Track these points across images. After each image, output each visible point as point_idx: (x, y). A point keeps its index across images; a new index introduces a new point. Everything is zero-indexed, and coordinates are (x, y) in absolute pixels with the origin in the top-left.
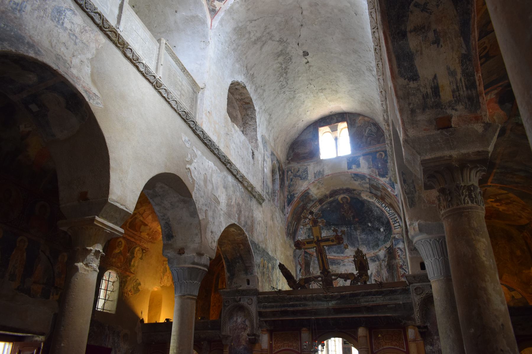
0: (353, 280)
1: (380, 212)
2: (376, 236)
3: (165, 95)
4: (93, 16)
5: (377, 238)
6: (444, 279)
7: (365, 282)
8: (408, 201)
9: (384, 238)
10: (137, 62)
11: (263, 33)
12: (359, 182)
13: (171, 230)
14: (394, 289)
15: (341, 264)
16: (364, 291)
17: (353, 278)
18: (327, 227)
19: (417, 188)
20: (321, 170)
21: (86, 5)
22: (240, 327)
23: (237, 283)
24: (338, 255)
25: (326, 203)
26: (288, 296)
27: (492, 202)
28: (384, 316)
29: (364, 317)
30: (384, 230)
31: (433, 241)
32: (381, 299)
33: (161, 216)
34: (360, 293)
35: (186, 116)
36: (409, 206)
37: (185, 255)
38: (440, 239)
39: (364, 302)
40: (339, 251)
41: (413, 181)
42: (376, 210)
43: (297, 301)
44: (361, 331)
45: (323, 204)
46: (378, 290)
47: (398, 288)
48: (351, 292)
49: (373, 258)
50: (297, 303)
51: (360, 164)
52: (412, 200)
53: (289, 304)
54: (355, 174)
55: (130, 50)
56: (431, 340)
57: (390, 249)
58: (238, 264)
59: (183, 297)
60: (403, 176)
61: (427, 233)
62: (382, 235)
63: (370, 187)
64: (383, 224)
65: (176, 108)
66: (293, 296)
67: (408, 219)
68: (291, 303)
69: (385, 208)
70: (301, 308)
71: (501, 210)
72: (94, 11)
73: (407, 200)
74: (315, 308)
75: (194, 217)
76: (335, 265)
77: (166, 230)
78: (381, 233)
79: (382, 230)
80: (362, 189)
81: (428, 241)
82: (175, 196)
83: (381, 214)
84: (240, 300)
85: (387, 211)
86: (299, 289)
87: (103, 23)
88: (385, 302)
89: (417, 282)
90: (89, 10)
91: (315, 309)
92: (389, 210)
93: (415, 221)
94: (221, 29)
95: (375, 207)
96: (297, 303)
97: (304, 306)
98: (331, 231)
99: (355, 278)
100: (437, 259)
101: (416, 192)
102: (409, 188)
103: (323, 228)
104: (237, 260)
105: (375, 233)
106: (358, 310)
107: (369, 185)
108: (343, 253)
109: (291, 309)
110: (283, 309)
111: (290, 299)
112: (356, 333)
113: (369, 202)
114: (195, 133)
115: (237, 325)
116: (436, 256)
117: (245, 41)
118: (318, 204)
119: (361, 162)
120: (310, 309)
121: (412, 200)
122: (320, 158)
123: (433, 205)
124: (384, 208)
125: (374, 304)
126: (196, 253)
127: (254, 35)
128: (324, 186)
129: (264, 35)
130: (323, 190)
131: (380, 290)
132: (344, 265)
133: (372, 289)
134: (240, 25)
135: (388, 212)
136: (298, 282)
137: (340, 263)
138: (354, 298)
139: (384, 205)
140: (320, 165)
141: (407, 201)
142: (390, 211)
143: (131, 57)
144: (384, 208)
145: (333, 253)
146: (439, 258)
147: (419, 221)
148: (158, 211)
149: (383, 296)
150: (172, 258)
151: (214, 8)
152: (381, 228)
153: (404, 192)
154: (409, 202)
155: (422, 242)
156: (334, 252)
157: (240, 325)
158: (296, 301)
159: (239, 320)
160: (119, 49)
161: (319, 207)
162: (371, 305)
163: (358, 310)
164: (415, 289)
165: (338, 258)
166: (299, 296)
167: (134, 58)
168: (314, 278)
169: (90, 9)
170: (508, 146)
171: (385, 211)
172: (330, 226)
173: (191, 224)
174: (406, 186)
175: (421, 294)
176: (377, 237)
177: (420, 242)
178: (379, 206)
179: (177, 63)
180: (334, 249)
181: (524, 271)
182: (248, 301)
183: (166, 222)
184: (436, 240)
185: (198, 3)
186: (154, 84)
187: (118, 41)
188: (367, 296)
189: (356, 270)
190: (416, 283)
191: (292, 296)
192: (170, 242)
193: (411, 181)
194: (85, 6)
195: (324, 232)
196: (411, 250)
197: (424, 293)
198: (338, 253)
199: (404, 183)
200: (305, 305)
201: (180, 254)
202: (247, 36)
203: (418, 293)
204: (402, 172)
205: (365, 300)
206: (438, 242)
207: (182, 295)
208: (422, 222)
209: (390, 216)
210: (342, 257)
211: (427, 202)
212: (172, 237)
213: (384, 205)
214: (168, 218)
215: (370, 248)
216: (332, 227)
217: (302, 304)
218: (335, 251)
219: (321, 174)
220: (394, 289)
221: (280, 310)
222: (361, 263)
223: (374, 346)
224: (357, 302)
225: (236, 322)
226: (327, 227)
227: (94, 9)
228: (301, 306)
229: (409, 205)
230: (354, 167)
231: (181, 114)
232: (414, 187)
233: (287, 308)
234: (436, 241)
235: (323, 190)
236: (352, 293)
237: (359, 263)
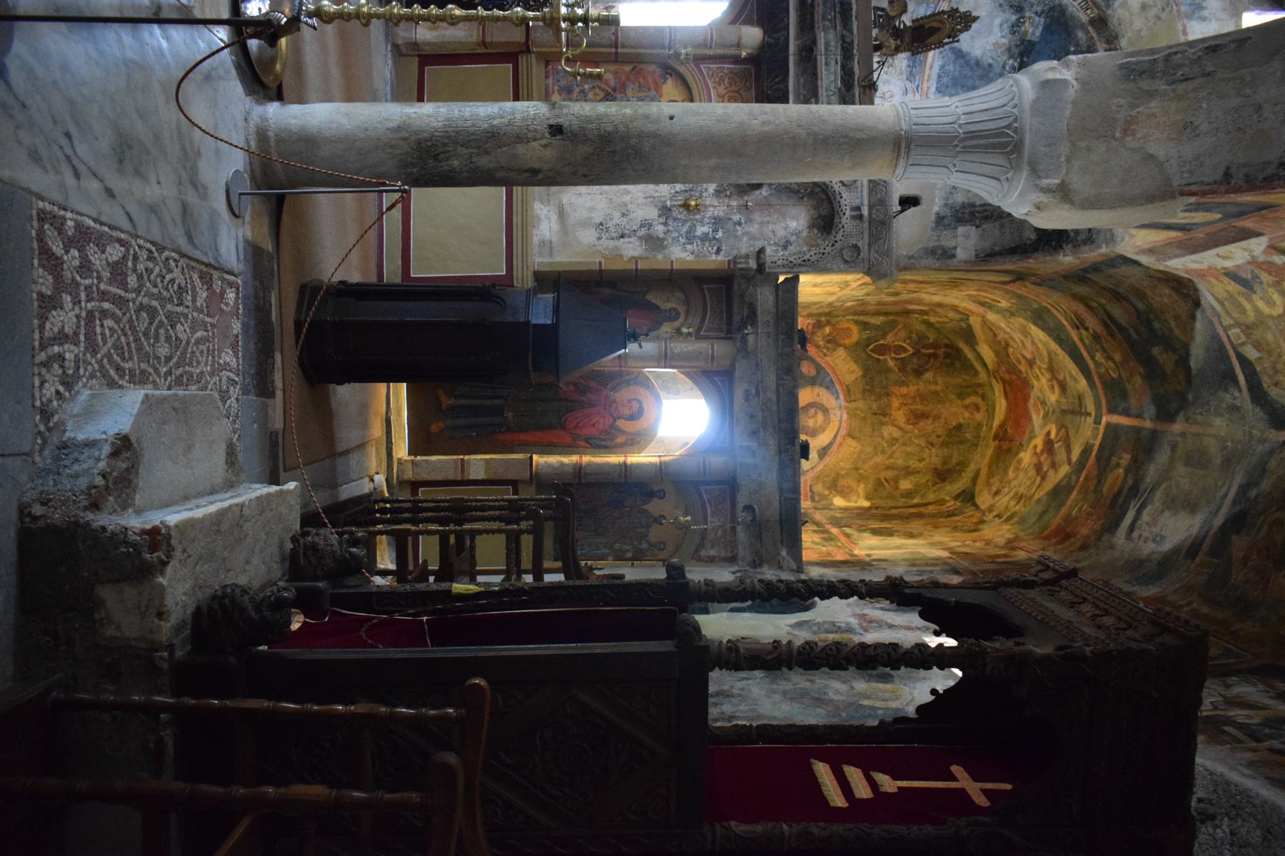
0: (887, 13)
6: (902, 130)
7: (877, 48)
8: (1143, 61)
15: (909, 85)
16: (856, 42)
17: (893, 14)
18: (1017, 46)
19: (1181, 87)
20: (1205, 13)
24: (934, 77)
25: (1092, 38)
27: (1049, 433)
28: (788, 91)
29: (787, 39)
31: (1012, 112)
32: (833, 85)
34: (851, 31)
36: (1124, 61)
38: (1016, 131)
39: (826, 39)
40: (945, 80)
41: (1209, 74)
44: (753, 35)
45: (1090, 28)
46: (856, 78)
48: (854, 7)
52: (1144, 72)
56: (728, 194)
60: (1233, 41)
61: (1035, 102)
71: (1022, 455)
73: (1146, 58)
76: (909, 66)
81: (1013, 99)
88: (825, 94)
93: (1077, 73)
98: (1005, 58)
99: (893, 18)
100: (959, 118)
102: (1187, 62)
103: (1015, 32)
106: (807, 25)
108: (939, 92)
112: (748, 22)
116: (966, 119)
118: (1093, 13)
121: (1144, 72)
122: (1247, 9)
123: (1118, 130)
125: (819, 63)
128: (1150, 24)
130: (1138, 23)
131: (856, 82)
132: (906, 92)
137: (911, 81)
138: (838, 15)
140: (1224, 9)
145: (940, 63)
146: (960, 126)
147: (1075, 83)
149: (839, 89)
153: (1174, 50)
154: (1137, 63)
156: (942, 67)
161: (1083, 17)
162: (819, 57)
163: (807, 25)
165: (926, 77)
170: (1229, 444)
172: (1019, 54)
174: (1194, 54)
180: (951, 67)
181: (862, 486)
184: (1015, 120)
188: (843, 48)
189: (913, 21)
193: (1210, 68)
195: (1003, 37)
197: (842, 188)
198: (939, 77)
199: (1207, 48)
205: (832, 43)
206: (1008, 127)
208: (1071, 93)
210: (928, 88)
211: (1134, 113)
216: (1015, 61)
218: (947, 67)
219: (1194, 12)
222: (933, 31)
223: (716, 66)
224: (827, 23)
226: (1017, 46)
229: (1128, 63)
232: (1186, 80)
234: (1012, 119)
235: (1138, 23)
236: (851, 9)
237: (935, 24)
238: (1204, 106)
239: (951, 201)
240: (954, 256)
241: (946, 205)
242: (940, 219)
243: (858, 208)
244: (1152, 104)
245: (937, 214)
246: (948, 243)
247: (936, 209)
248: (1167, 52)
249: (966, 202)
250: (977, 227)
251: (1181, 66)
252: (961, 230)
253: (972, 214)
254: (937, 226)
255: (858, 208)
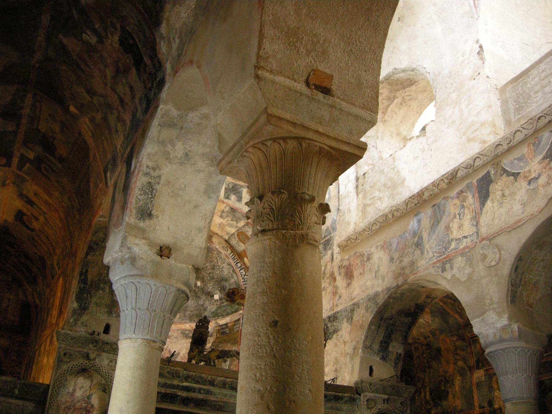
1: (229, 272)
2: (202, 303)
5: (203, 305)
8: (511, 295)
9: (216, 310)
12: (224, 222)
13: (151, 201)
14: (340, 394)
19: (523, 283)
22: (78, 405)
23: (86, 326)
26: (185, 372)
30: (221, 299)
33: (147, 167)
37: (172, 261)
42: (223, 267)
43: (197, 382)
47: (346, 395)
49: (187, 332)
50: (195, 385)
51: (242, 197)
53: (181, 384)
54: (232, 209)
57: (224, 327)
58: (101, 292)
59: (153, 344)
62: (213, 305)
63: (234, 233)
64: (222, 289)
66: (194, 374)
67: (508, 318)
68: (185, 384)
69: (241, 270)
70: (200, 396)
73: (510, 293)
74: (224, 400)
75: (210, 197)
77: (141, 197)
78: (213, 301)
79: (216, 297)
80: (219, 232)
82: (209, 143)
83: (230, 275)
84: (94, 359)
85: (241, 275)
86: (202, 364)
89: (371, 391)
91: (224, 402)
92: (244, 274)
93: (514, 322)
95: (224, 263)
96: (195, 385)
97: (206, 394)
101: (520, 286)
104: (102, 285)
105: (204, 297)
107: (238, 230)
109: (184, 394)
110: (169, 391)
111: (187, 378)
113: (219, 253)
115: (72, 401)
119: (243, 196)
120: (216, 401)
124: (239, 269)
126: (193, 266)
133: (345, 393)
135: (243, 276)
136: (205, 353)
139: (239, 265)
141: (509, 294)
142: (246, 277)
144: (239, 269)
147: (518, 324)
148: (148, 154)
150: (142, 258)
152: (216, 294)
153: (510, 282)
155: (516, 350)
157: (79, 401)
158: (196, 383)
159: (79, 394)
164: (367, 401)
166: (203, 375)
168: (235, 353)
171: (240, 274)
173: (196, 207)
175: (372, 408)
176: (204, 304)
177: (514, 350)
178: (233, 264)
182: (111, 364)
183: (150, 183)
190: (370, 392)
191: (191, 373)
192: (142, 224)
193: (521, 272)
196: (366, 348)
197: (376, 407)
200: (208, 392)
201: (161, 256)
203: (370, 406)
204: (520, 257)
207: (152, 339)
208: (521, 326)
209: (244, 283)
211: (525, 303)
212: (150, 215)
213: (239, 265)
214: (159, 177)
215: (185, 316)
217: (204, 390)
220: (340, 394)
221: (163, 391)
225: (72, 394)
228: (201, 393)
230: (233, 197)
233: (177, 391)
238: (531, 276)
239: (377, 351)
240: (400, 354)
241: (378, 354)
242: (384, 358)
243: (384, 400)
244: (524, 294)
245: (380, 359)
246: (393, 356)
247: (378, 359)
248: (510, 285)
249: (379, 344)
250: (392, 341)
251: (516, 281)
252: (390, 349)
253: (385, 342)
254: (386, 360)
255: (384, 400)
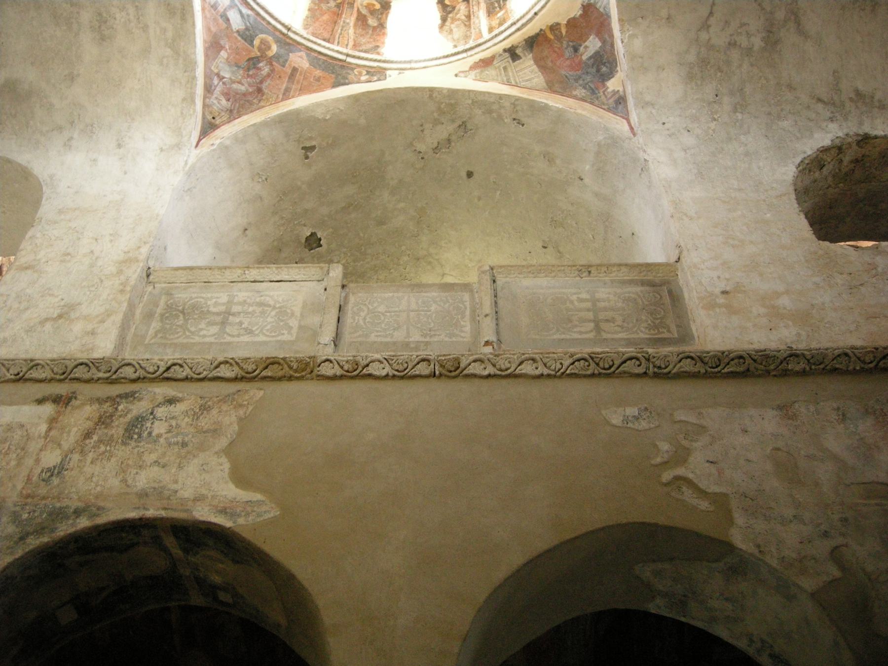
3: (490, 370)
4: (215, 375)
10: (360, 369)
11: (763, 9)
21: (193, 370)
35: (593, 365)
55: (327, 363)
65: (546, 371)
72: (212, 367)
87: (242, 368)
90: (205, 373)
94: (654, 111)
114: (669, 378)
117: (745, 66)
127: (749, 35)
129: (768, 9)
134: (691, 57)
143: (339, 372)
151: (617, 96)
160: (307, 379)
167: (346, 368)
169: (204, 370)
179: (553, 274)
185: (579, 126)
186: (437, 373)
187: (291, 368)
194: (194, 373)
202: (735, 54)
227: (209, 363)
231: (576, 372)
